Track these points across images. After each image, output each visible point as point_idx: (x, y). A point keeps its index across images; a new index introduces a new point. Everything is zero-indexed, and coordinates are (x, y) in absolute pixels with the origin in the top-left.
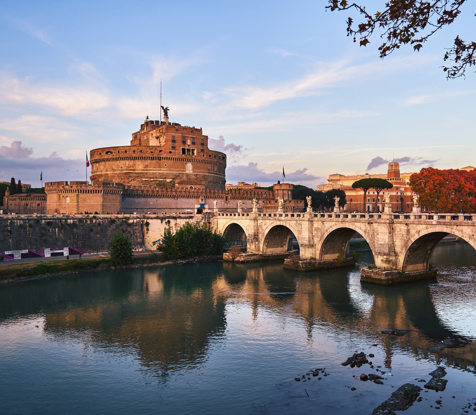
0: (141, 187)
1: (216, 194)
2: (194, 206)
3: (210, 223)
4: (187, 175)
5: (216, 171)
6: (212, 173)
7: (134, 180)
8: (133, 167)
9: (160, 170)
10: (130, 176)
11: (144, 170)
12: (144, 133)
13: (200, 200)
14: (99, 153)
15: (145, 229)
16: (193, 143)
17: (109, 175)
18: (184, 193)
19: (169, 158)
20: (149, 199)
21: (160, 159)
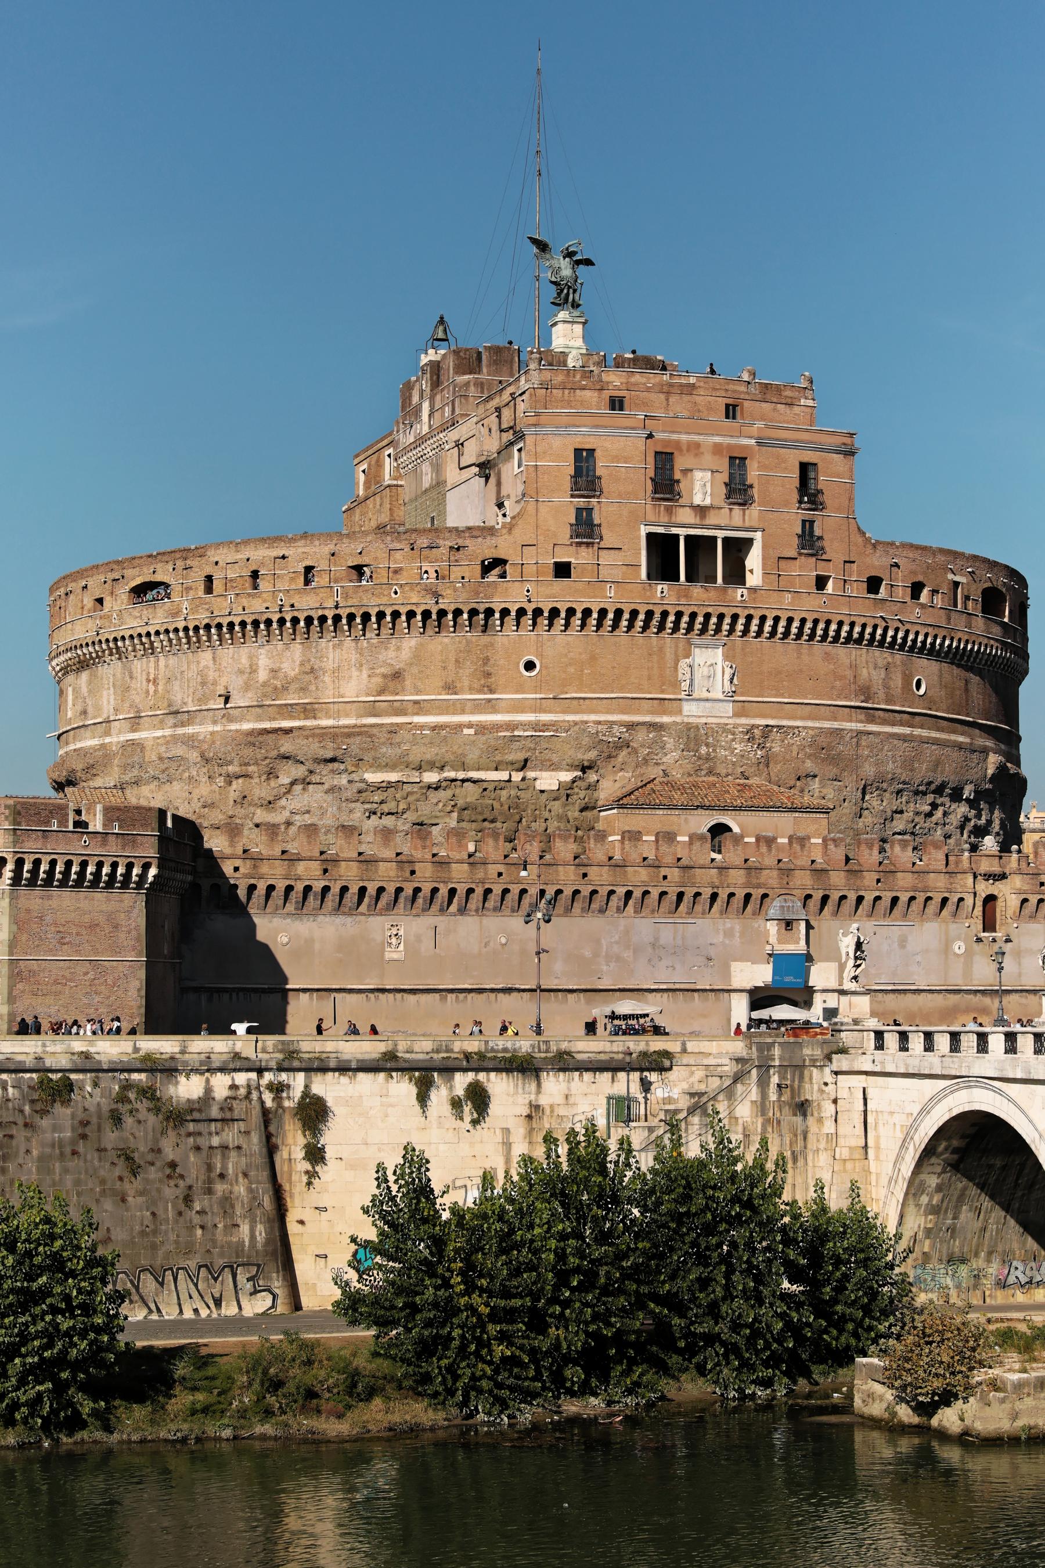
0: (349, 830)
1: (905, 880)
2: (727, 974)
3: (802, 1108)
4: (693, 736)
6: (892, 716)
7: (306, 783)
8: (303, 690)
9: (490, 706)
10: (286, 757)
12: (421, 440)
13: (772, 928)
14: (88, 602)
15: (294, 1143)
17: (151, 756)
18: (643, 874)
19: (554, 613)
20: (378, 926)
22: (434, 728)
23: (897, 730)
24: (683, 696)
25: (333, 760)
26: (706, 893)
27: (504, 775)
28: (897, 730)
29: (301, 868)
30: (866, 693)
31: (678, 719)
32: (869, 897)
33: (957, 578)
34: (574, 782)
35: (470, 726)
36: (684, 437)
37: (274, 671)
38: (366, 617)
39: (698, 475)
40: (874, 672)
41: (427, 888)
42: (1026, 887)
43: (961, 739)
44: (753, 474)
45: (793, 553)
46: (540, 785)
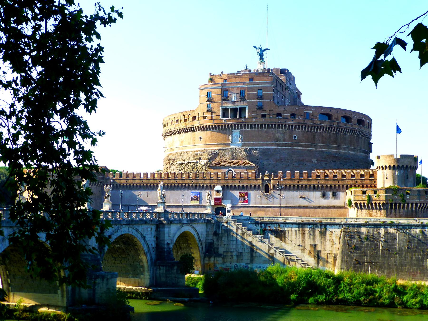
4: (232, 151)
5: (298, 141)
10: (170, 160)
16: (242, 98)
19: (203, 126)
21: (193, 130)
23: (286, 148)
24: (230, 143)
25: (175, 160)
26: (201, 185)
28: (286, 148)
29: (122, 181)
30: (277, 140)
31: (229, 147)
32: (237, 185)
34: (207, 162)
40: (279, 135)
41: (145, 185)
42: (274, 183)
43: (311, 149)
44: (246, 93)
45: (255, 110)
46: (202, 163)
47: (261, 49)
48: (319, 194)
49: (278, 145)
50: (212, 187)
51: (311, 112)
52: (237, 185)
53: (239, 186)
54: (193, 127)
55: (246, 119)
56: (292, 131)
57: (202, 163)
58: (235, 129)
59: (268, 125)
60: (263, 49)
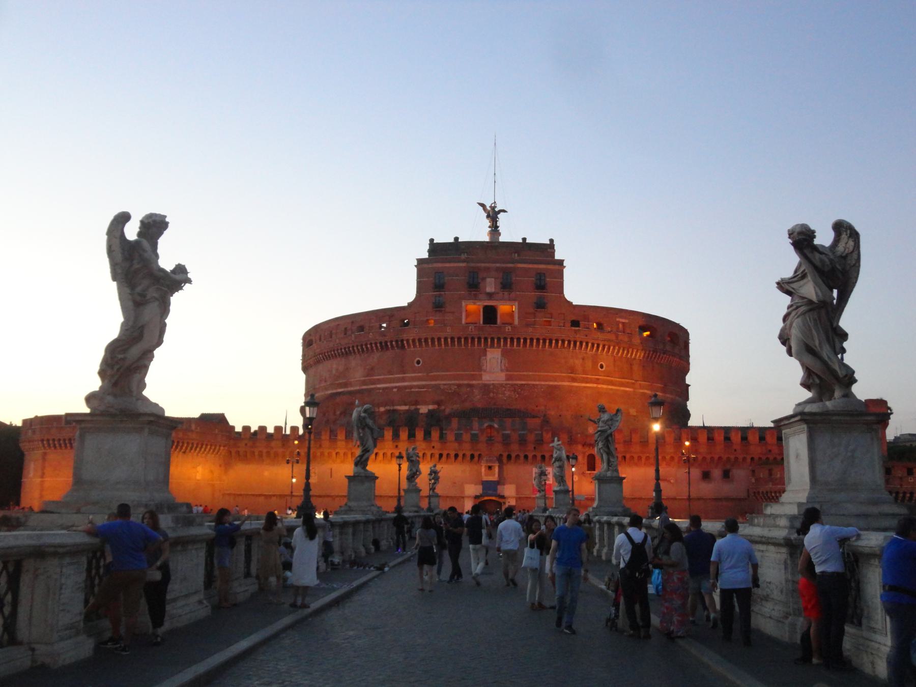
2: (463, 492)
4: (486, 388)
9: (403, 380)
11: (364, 383)
13: (483, 470)
22: (384, 389)
23: (588, 385)
26: (453, 453)
27: (407, 408)
28: (588, 385)
30: (572, 370)
33: (624, 321)
35: (396, 387)
36: (483, 265)
37: (337, 370)
38: (362, 346)
39: (488, 280)
46: (421, 411)
47: (493, 208)
48: (696, 473)
49: (574, 380)
50: (476, 458)
51: (627, 321)
52: (530, 456)
53: (535, 457)
54: (402, 341)
55: (514, 328)
56: (596, 355)
57: (421, 411)
58: (492, 346)
59: (557, 341)
60: (497, 210)
